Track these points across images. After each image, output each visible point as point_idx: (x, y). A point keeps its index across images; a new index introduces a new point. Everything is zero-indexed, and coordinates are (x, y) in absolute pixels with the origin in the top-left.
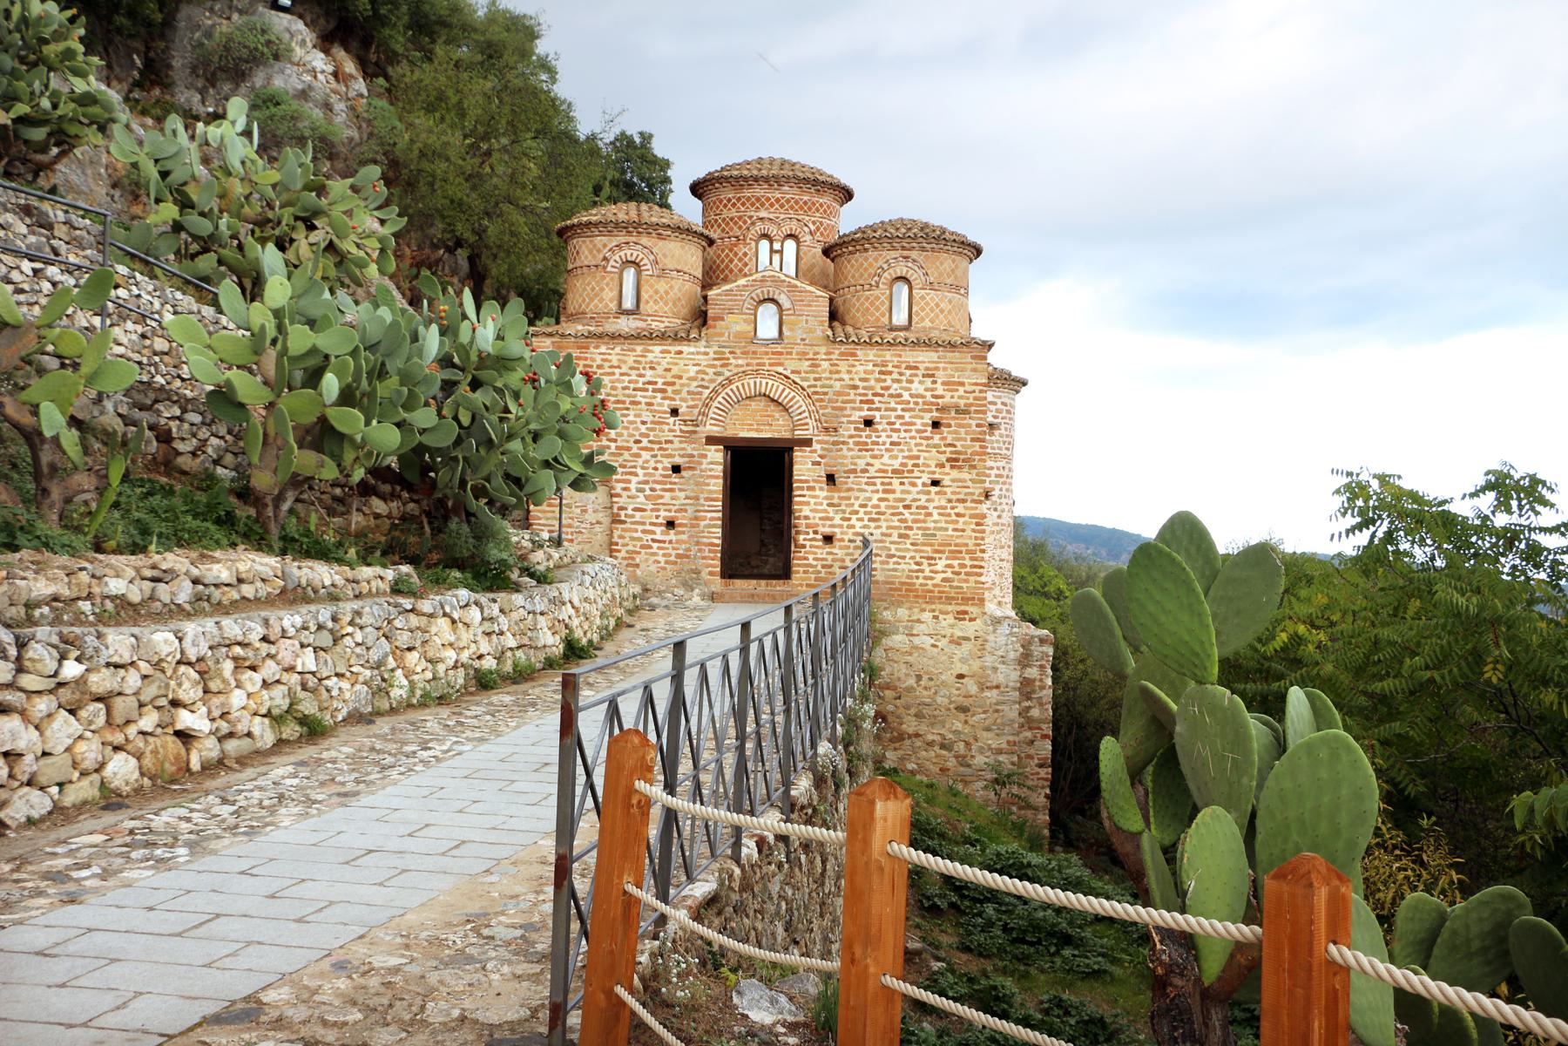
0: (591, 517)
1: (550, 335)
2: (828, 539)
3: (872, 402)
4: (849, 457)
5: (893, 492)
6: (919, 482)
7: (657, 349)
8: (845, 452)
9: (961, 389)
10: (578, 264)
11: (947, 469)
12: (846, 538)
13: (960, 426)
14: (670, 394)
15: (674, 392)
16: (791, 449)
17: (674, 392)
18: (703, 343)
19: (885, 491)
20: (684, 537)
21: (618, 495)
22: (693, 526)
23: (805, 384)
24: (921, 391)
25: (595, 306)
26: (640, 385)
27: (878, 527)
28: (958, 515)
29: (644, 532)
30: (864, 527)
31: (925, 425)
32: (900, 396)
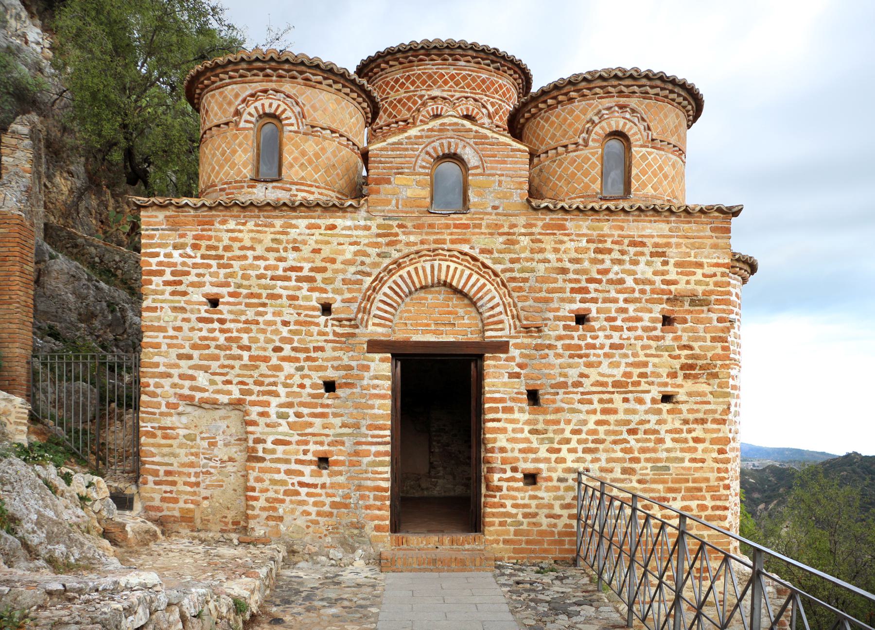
0: (221, 452)
1: (162, 207)
2: (531, 478)
3: (586, 291)
4: (557, 366)
5: (615, 411)
6: (647, 397)
7: (302, 223)
8: (552, 359)
9: (699, 272)
10: (208, 125)
11: (679, 380)
12: (555, 476)
13: (698, 321)
14: (319, 284)
15: (324, 280)
16: (480, 357)
17: (324, 280)
18: (363, 213)
19: (604, 411)
20: (341, 479)
21: (254, 423)
22: (352, 464)
23: (498, 268)
24: (649, 275)
25: (227, 173)
26: (280, 272)
27: (596, 460)
28: (696, 440)
29: (288, 472)
30: (578, 460)
31: (653, 320)
32: (621, 281)
